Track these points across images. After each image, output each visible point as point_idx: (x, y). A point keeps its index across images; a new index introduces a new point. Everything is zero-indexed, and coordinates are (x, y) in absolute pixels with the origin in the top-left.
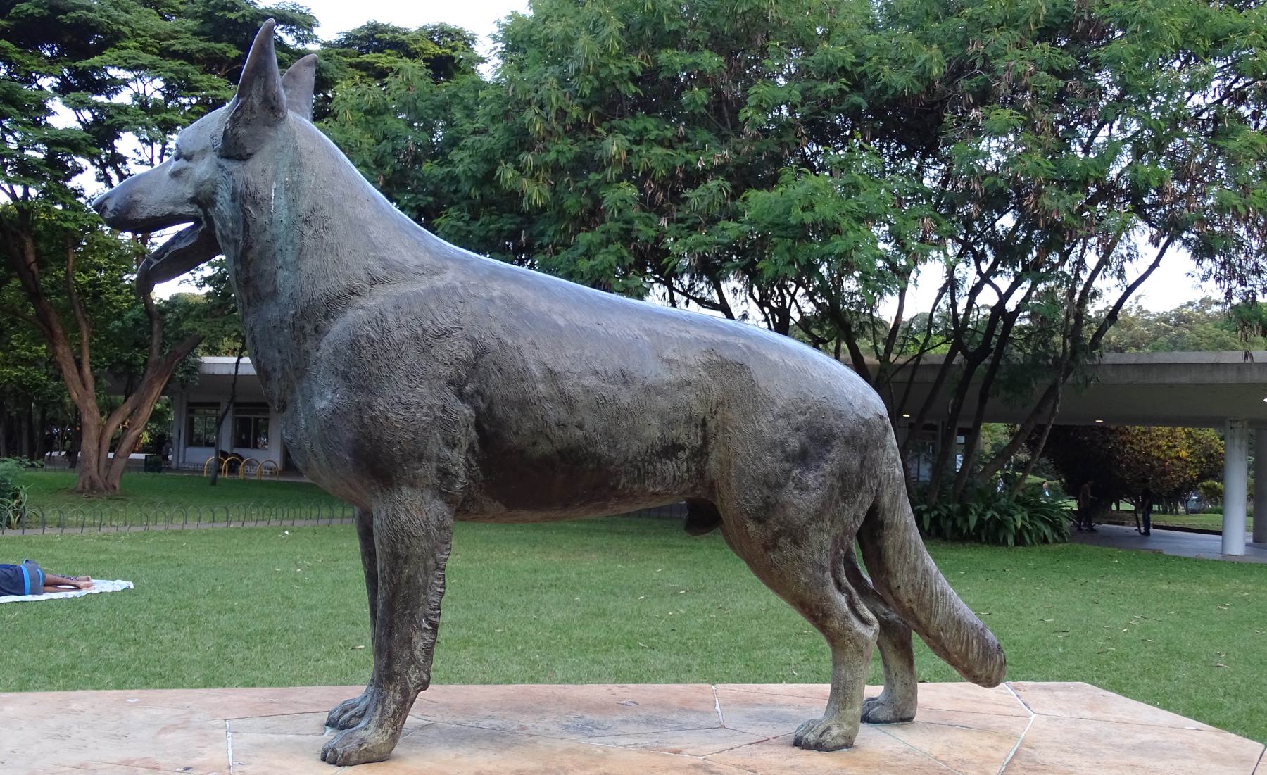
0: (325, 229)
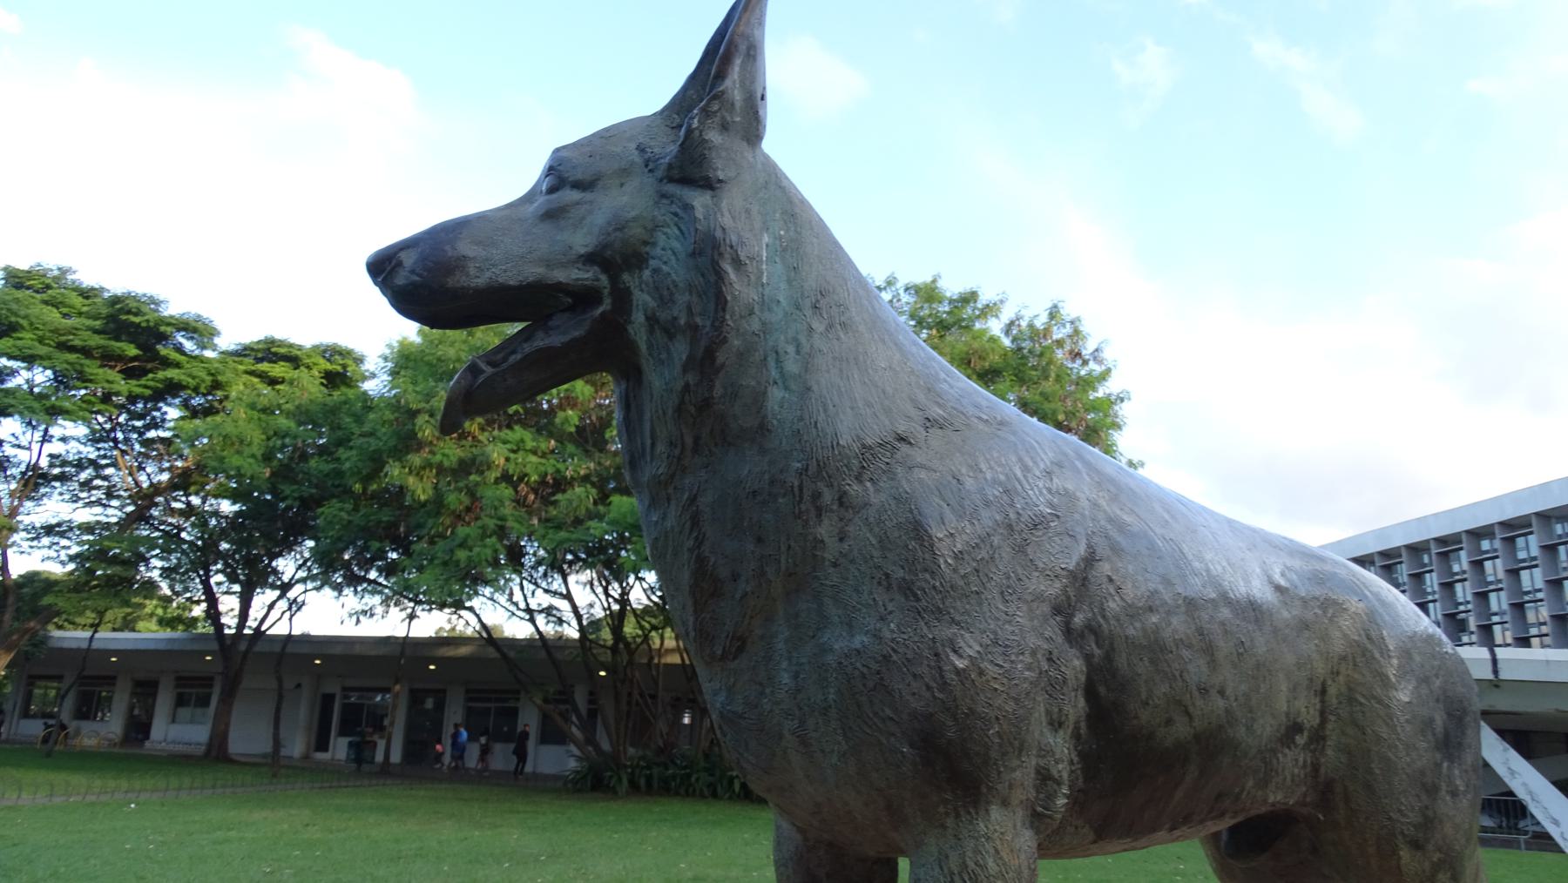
0: (843, 325)
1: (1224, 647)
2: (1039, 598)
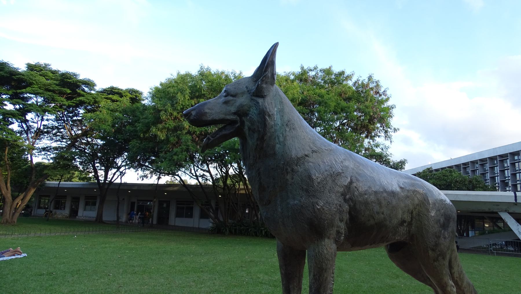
0: (293, 129)
1: (384, 203)
2: (338, 192)
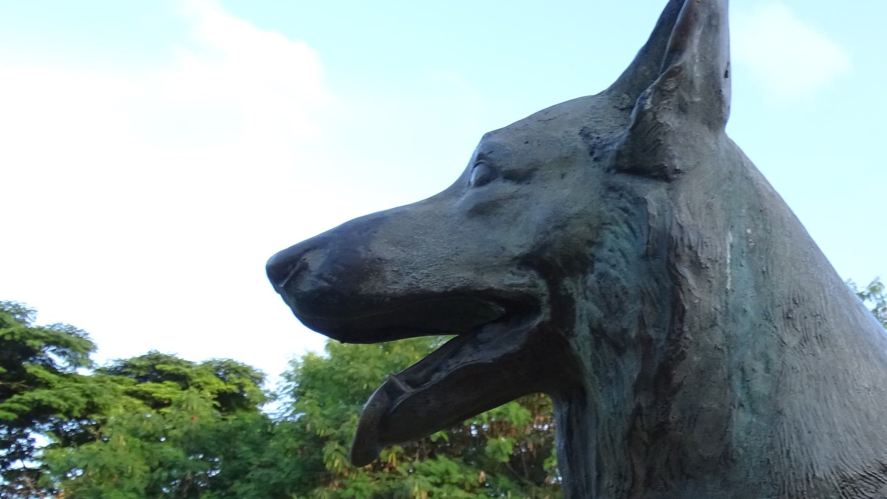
0: (820, 338)
